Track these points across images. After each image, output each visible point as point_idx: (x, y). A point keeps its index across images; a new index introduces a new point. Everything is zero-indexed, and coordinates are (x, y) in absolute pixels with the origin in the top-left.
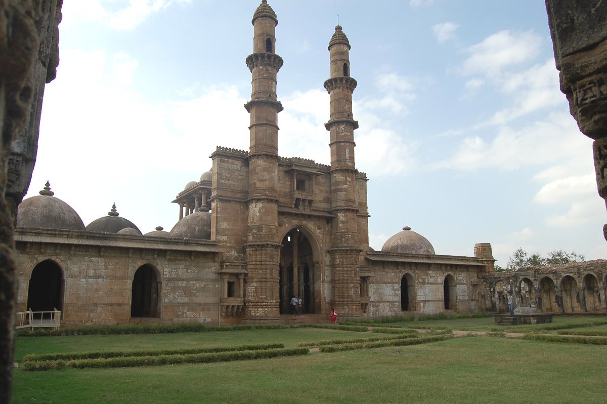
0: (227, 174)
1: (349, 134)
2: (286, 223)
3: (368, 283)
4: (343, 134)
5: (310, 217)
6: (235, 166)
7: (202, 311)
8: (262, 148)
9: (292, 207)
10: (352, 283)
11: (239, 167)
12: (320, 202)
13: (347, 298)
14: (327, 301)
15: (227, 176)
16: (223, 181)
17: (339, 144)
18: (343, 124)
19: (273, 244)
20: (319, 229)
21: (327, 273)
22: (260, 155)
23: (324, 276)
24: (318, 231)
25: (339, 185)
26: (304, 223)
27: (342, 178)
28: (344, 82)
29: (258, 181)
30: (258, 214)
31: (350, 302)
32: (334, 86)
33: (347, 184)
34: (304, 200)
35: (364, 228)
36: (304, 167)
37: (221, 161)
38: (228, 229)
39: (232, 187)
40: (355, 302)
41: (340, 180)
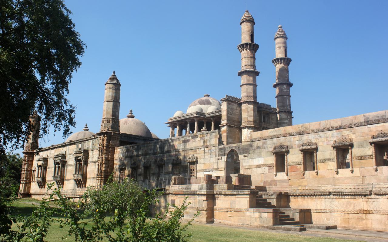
1: (288, 91)
4: (285, 91)
6: (234, 107)
8: (251, 97)
11: (236, 107)
16: (229, 115)
17: (283, 96)
18: (285, 85)
22: (251, 102)
25: (283, 120)
27: (285, 116)
28: (286, 60)
29: (249, 116)
30: (249, 135)
32: (280, 62)
33: (287, 120)
36: (267, 109)
37: (228, 104)
41: (284, 117)
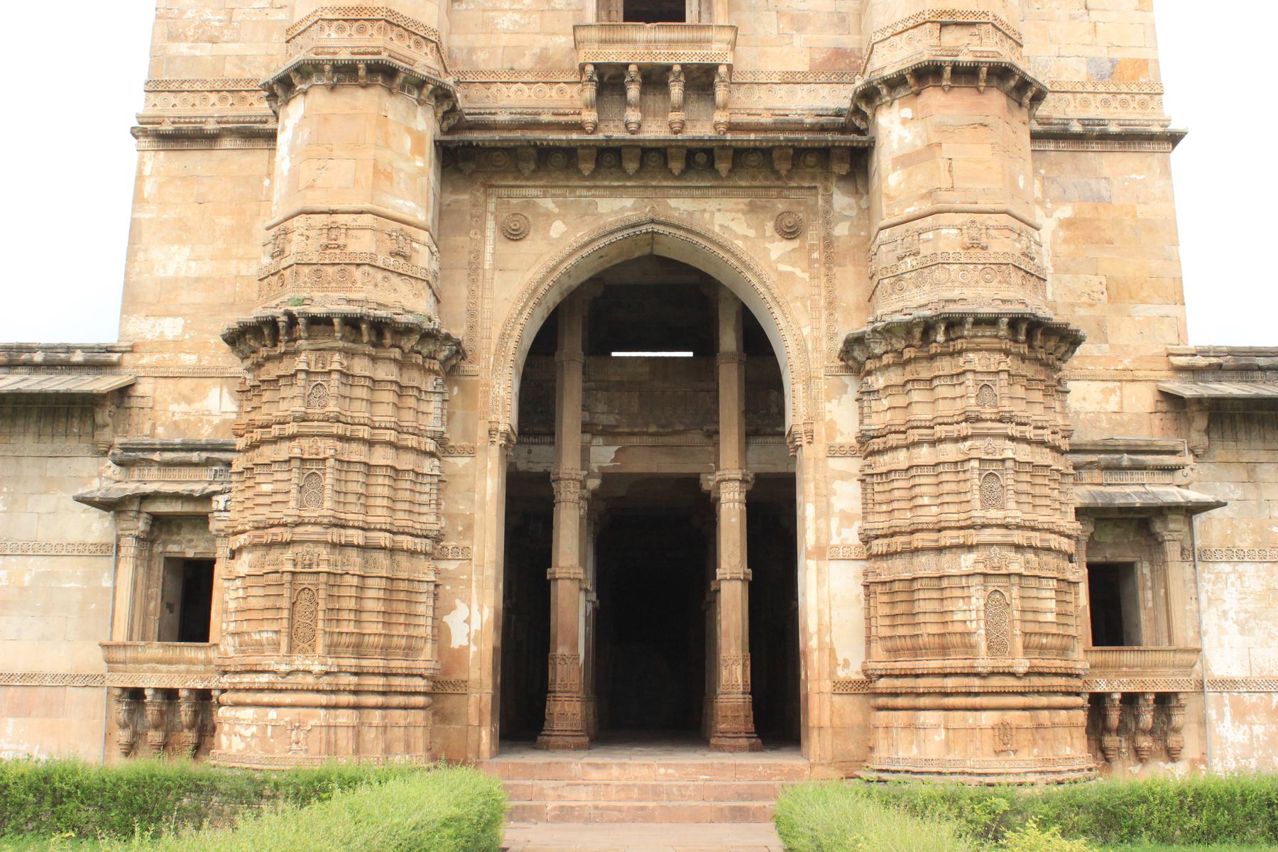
0: (208, 14)
2: (549, 216)
3: (1172, 550)
5: (700, 162)
7: (16, 715)
9: (579, 127)
10: (970, 548)
12: (790, 80)
13: (944, 650)
14: (842, 674)
15: (205, 22)
16: (182, 48)
19: (316, 310)
20: (790, 233)
21: (847, 496)
23: (824, 513)
24: (779, 248)
31: (950, 683)
34: (655, 78)
35: (1140, 208)
38: (197, 280)
39: (231, 71)
40: (995, 683)
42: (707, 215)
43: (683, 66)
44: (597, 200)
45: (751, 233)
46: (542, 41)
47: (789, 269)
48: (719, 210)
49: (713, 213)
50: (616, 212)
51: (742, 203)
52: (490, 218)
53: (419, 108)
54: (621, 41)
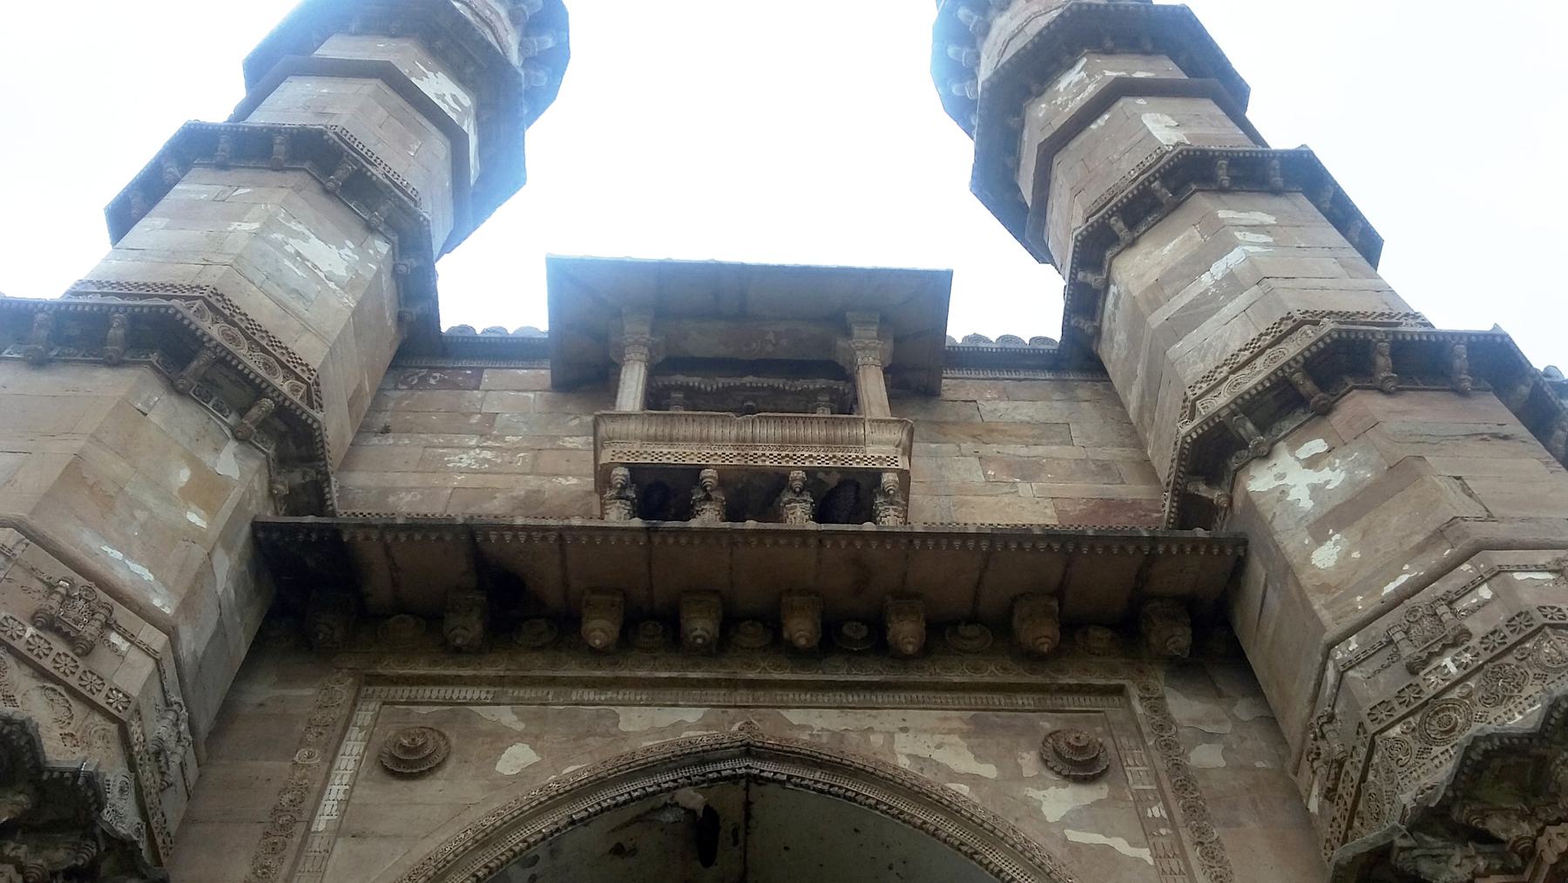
2: (500, 739)
20: (1081, 766)
24: (1058, 801)
26: (813, 723)
42: (877, 740)
43: (810, 472)
44: (619, 709)
45: (989, 771)
46: (533, 482)
47: (1099, 839)
48: (904, 730)
49: (892, 735)
50: (661, 731)
51: (956, 719)
52: (354, 733)
53: (232, 445)
54: (685, 439)
